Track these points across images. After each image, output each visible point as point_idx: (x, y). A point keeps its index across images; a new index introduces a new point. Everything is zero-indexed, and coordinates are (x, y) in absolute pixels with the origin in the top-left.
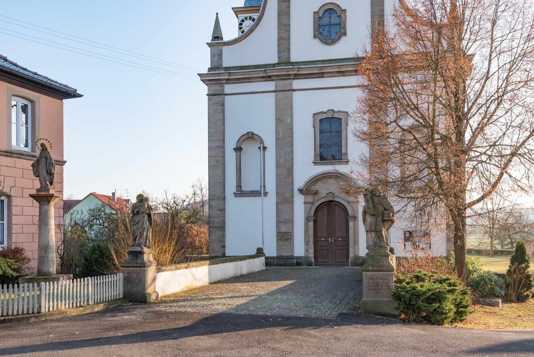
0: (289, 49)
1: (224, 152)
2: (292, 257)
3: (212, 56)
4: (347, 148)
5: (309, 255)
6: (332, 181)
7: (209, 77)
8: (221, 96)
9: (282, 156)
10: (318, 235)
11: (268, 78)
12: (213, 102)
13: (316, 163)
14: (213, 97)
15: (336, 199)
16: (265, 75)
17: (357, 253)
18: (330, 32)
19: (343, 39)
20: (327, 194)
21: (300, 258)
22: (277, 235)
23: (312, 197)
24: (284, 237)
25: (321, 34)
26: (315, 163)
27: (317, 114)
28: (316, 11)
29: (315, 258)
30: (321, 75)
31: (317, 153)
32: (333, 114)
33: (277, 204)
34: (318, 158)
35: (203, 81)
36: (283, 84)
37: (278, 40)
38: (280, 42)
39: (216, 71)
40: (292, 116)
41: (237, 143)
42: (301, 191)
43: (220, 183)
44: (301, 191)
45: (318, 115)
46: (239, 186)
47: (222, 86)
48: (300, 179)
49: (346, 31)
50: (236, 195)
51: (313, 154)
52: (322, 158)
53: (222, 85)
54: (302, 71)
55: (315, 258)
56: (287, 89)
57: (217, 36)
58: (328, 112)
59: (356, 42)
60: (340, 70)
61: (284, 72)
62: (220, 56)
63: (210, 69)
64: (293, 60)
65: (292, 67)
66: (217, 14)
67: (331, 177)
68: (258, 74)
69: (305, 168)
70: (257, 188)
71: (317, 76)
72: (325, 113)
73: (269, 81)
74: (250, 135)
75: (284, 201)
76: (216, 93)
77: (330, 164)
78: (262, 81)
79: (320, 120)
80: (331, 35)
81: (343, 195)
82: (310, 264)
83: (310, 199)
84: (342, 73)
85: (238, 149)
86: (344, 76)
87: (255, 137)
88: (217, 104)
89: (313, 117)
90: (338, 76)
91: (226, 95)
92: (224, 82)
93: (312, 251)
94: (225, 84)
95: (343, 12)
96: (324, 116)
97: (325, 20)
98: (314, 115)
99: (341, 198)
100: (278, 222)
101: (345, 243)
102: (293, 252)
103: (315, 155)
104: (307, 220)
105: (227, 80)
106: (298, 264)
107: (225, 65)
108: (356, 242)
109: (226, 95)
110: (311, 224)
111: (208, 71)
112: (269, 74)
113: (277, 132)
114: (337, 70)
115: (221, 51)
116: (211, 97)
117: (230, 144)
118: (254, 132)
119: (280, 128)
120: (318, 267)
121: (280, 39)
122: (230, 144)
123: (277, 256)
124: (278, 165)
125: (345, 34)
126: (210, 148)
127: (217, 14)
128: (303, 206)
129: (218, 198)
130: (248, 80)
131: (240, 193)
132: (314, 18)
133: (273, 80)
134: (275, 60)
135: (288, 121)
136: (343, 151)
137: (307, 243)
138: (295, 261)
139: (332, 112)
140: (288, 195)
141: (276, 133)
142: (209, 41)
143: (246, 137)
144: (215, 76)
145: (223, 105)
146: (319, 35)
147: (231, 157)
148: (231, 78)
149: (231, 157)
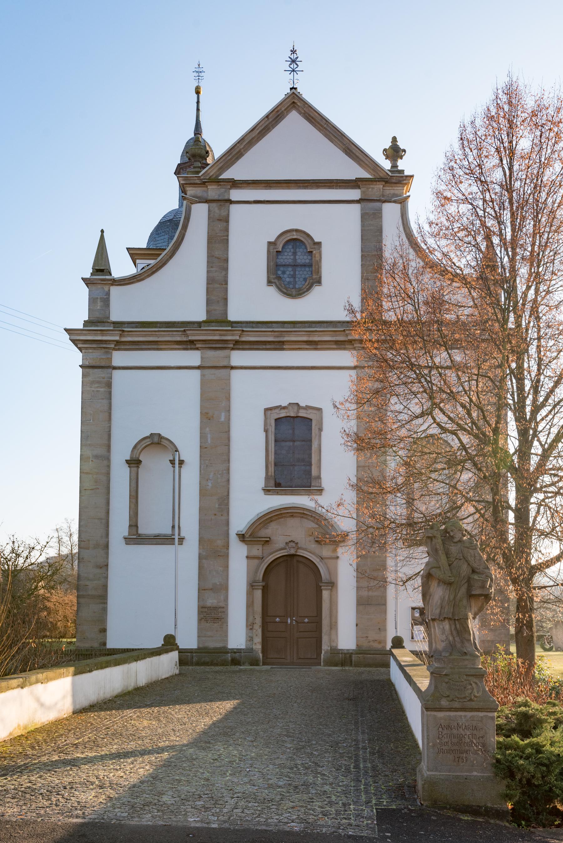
0: (226, 300)
1: (109, 466)
2: (224, 650)
3: (92, 301)
4: (319, 467)
5: (254, 647)
6: (292, 522)
7: (85, 335)
8: (106, 370)
9: (211, 476)
11: (190, 345)
12: (90, 378)
14: (91, 371)
15: (301, 553)
16: (185, 339)
17: (334, 644)
18: (294, 276)
19: (316, 289)
21: (239, 651)
22: (200, 612)
23: (260, 547)
24: (212, 615)
25: (279, 278)
26: (267, 491)
27: (270, 409)
28: (273, 240)
29: (263, 652)
30: (279, 346)
31: (270, 474)
32: (298, 412)
33: (201, 558)
34: (272, 483)
35: (73, 341)
36: (215, 356)
37: (208, 284)
38: (210, 286)
39: (97, 326)
40: (228, 410)
41: (132, 451)
42: (242, 537)
43: (101, 519)
44: (242, 537)
45: (274, 411)
46: (134, 525)
48: (242, 516)
49: (320, 278)
50: (128, 541)
51: (263, 474)
52: (278, 485)
53: (108, 351)
54: (248, 336)
55: (264, 650)
56: (222, 364)
57: (101, 267)
58: (290, 408)
59: (336, 295)
60: (311, 339)
61: (216, 337)
62: (106, 301)
63: (86, 323)
64: (233, 316)
65: (230, 328)
66: (102, 231)
67: (292, 515)
68: (173, 336)
69: (249, 499)
70: (167, 531)
72: (284, 408)
73: (191, 349)
74: (156, 439)
75: (213, 553)
76: (98, 364)
77: (292, 493)
79: (276, 420)
80: (295, 282)
81: (313, 546)
82: (254, 662)
83: (257, 550)
84: (314, 345)
85: (134, 463)
86: (316, 349)
87: (164, 442)
88: (98, 382)
89: (265, 414)
90: (307, 349)
91: (115, 368)
92: (113, 346)
93: (258, 639)
94: (114, 349)
95: (316, 246)
96: (283, 414)
97: (287, 258)
98: (266, 410)
99: (310, 551)
100: (202, 590)
101: (315, 625)
102: (227, 641)
103: (267, 478)
104: (252, 586)
105: (118, 343)
106: (235, 662)
107: (114, 317)
108: (334, 625)
109: (115, 368)
110: (258, 594)
111: (85, 325)
112: (191, 338)
113: (203, 436)
114: (305, 339)
115: (108, 294)
116: (87, 370)
117: (121, 452)
118: (163, 434)
119: (208, 429)
120: (268, 667)
121: (210, 281)
122: (121, 452)
123: (199, 648)
124: (203, 492)
125: (319, 282)
126: (83, 458)
127: (102, 231)
128: (245, 562)
129: (96, 546)
130: (155, 345)
131: (136, 537)
132: (269, 252)
133: (197, 349)
134: (201, 316)
135: (223, 419)
136: (314, 473)
137: (250, 626)
140: (220, 543)
141: (201, 437)
142: (88, 275)
143: (148, 442)
144: (96, 335)
145: (109, 385)
146: (276, 281)
147: (120, 476)
148: (124, 339)
149: (120, 476)
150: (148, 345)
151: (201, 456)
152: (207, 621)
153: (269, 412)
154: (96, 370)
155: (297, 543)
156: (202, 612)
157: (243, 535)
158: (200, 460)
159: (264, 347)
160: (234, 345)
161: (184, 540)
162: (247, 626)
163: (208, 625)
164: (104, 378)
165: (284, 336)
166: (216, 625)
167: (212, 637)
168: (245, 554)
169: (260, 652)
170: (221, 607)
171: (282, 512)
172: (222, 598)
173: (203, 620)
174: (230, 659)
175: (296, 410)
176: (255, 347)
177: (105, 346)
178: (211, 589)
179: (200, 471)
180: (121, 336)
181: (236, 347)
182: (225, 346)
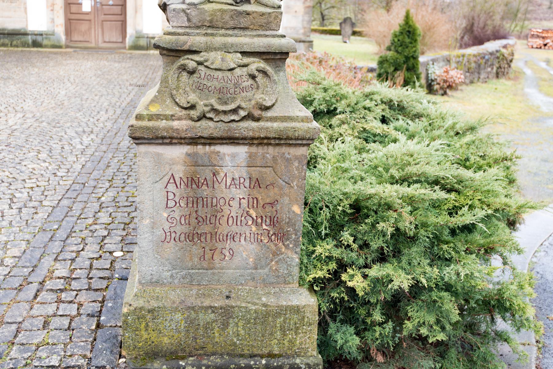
17: (139, 28)
93: (60, 20)
106: (36, 44)
138: (30, 39)
162: (47, 7)
163: (5, 4)
166: (13, 5)
167: (11, 17)
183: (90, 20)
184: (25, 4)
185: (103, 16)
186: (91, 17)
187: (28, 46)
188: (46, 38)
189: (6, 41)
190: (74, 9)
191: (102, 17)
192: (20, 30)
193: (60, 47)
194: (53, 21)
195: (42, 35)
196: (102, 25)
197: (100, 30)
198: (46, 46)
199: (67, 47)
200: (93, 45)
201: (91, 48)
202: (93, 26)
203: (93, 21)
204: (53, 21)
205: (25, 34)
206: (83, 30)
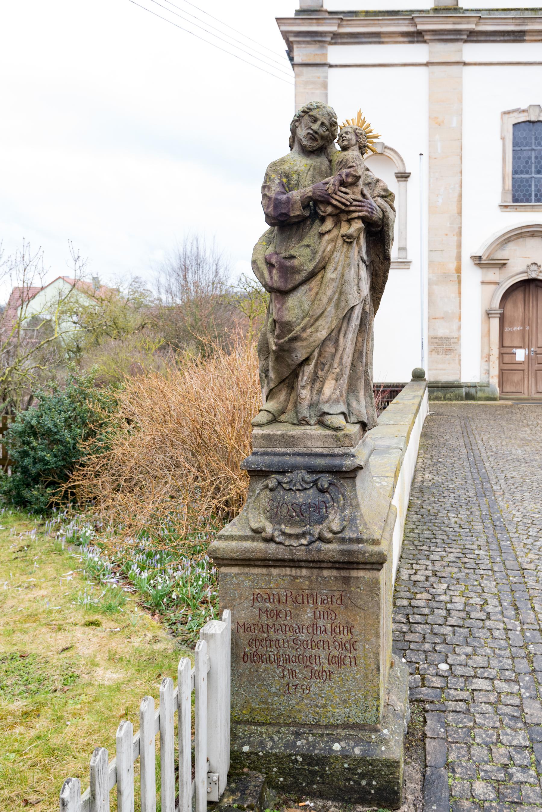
10: (507, 343)
11: (416, 37)
13: (506, 207)
16: (412, 29)
20: (528, 266)
22: (430, 343)
23: (496, 271)
24: (443, 345)
27: (508, 113)
29: (499, 387)
31: (507, 188)
32: (539, 116)
33: (430, 283)
34: (510, 198)
39: (310, 15)
44: (478, 261)
45: (511, 115)
47: (322, 47)
54: (485, 24)
55: (501, 383)
58: (531, 111)
63: (298, 12)
71: (512, 38)
72: (524, 111)
73: (418, 42)
78: (403, 42)
79: (514, 125)
83: (493, 275)
89: (502, 118)
92: (328, 39)
93: (495, 372)
94: (331, 44)
100: (432, 319)
103: (504, 191)
104: (489, 314)
106: (469, 397)
110: (495, 323)
111: (296, 14)
118: (387, 144)
124: (433, 210)
128: (479, 288)
130: (376, 38)
133: (425, 42)
138: (464, 391)
139: (537, 110)
145: (325, 86)
150: (369, 37)
151: (430, 168)
152: (438, 353)
153: (507, 116)
154: (310, 69)
155: (540, 266)
156: (432, 343)
157: (480, 257)
158: (429, 172)
159: (502, 38)
160: (468, 36)
161: (411, 264)
162: (482, 358)
163: (440, 356)
164: (319, 78)
165: (527, 25)
166: (448, 357)
168: (480, 280)
169: (497, 386)
170: (453, 338)
171: (523, 230)
172: (455, 327)
173: (434, 352)
174: (464, 393)
175: (537, 114)
176: (492, 38)
177: (320, 39)
178: (443, 318)
179: (429, 185)
180: (339, 26)
181: (469, 39)
182: (458, 37)
183: (523, 370)
184: (460, 355)
185: (537, 365)
186: (525, 367)
187: (462, 400)
188: (481, 390)
189: (440, 394)
190: (507, 359)
191: (537, 366)
192: (452, 383)
193: (494, 399)
194: (488, 372)
195: (476, 387)
196: (536, 374)
197: (533, 380)
198: (480, 399)
199: (501, 399)
200: (526, 396)
201: (524, 399)
202: (526, 376)
203: (526, 371)
204: (488, 372)
205: (460, 386)
206: (516, 381)
